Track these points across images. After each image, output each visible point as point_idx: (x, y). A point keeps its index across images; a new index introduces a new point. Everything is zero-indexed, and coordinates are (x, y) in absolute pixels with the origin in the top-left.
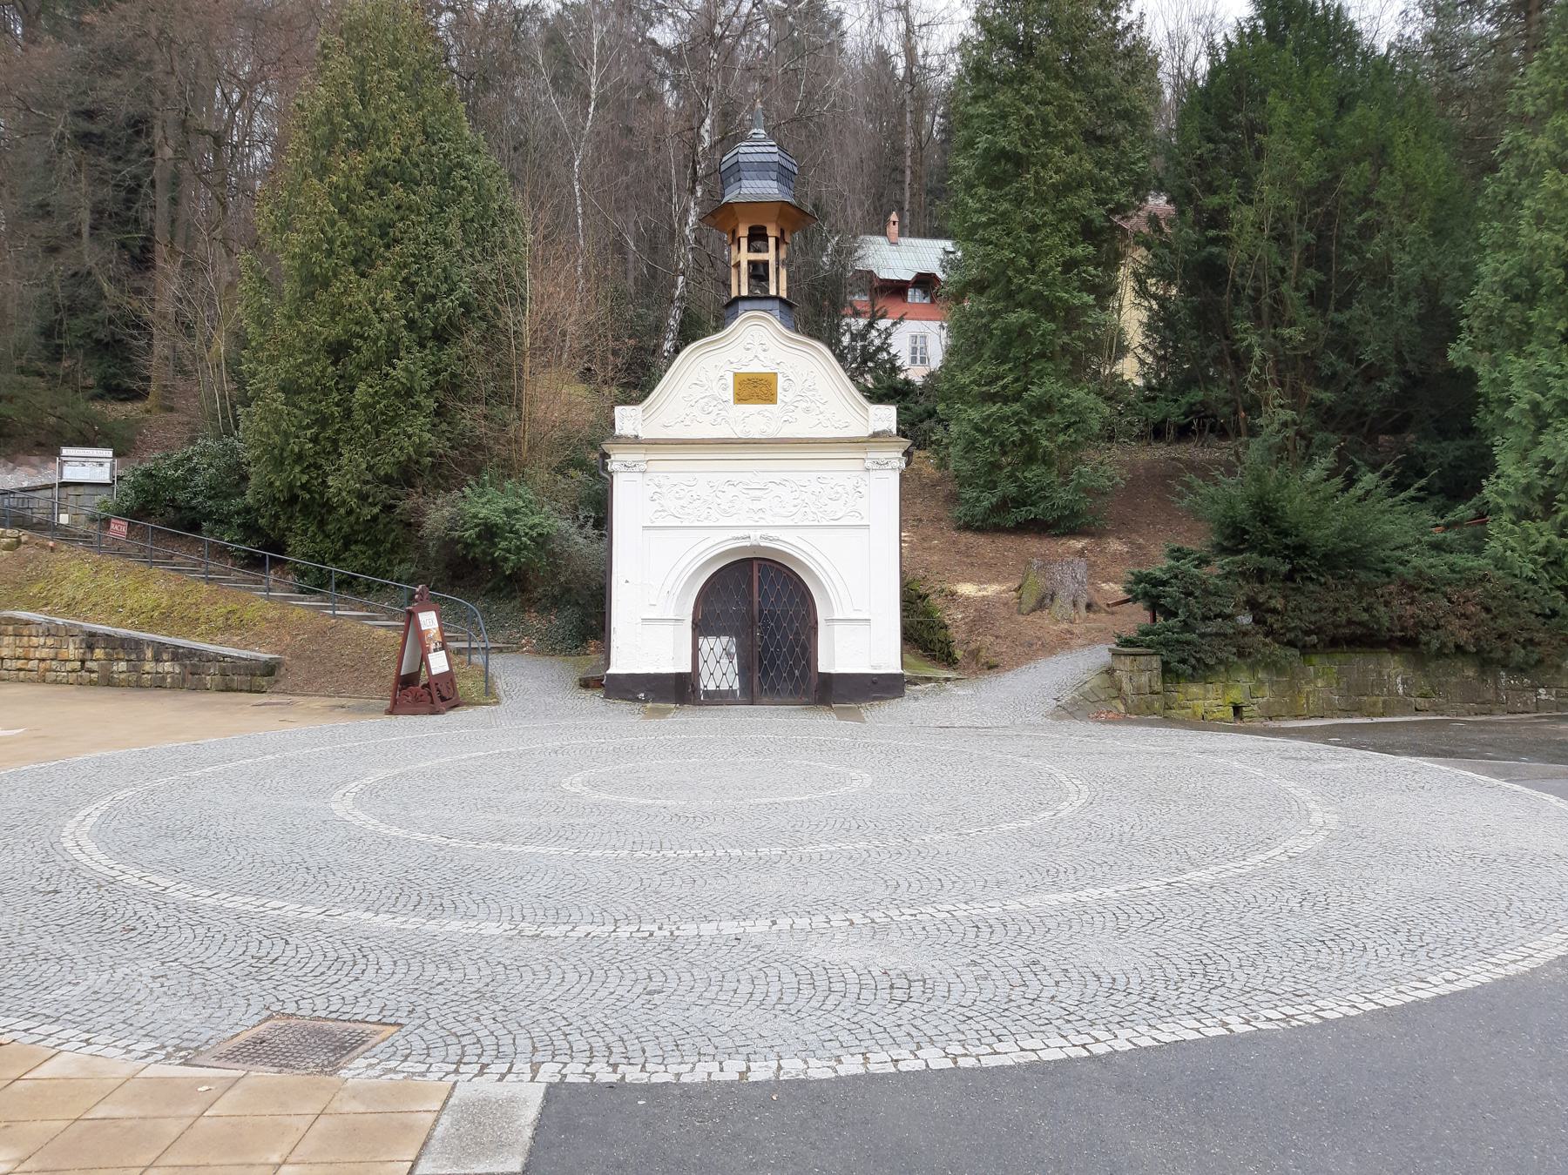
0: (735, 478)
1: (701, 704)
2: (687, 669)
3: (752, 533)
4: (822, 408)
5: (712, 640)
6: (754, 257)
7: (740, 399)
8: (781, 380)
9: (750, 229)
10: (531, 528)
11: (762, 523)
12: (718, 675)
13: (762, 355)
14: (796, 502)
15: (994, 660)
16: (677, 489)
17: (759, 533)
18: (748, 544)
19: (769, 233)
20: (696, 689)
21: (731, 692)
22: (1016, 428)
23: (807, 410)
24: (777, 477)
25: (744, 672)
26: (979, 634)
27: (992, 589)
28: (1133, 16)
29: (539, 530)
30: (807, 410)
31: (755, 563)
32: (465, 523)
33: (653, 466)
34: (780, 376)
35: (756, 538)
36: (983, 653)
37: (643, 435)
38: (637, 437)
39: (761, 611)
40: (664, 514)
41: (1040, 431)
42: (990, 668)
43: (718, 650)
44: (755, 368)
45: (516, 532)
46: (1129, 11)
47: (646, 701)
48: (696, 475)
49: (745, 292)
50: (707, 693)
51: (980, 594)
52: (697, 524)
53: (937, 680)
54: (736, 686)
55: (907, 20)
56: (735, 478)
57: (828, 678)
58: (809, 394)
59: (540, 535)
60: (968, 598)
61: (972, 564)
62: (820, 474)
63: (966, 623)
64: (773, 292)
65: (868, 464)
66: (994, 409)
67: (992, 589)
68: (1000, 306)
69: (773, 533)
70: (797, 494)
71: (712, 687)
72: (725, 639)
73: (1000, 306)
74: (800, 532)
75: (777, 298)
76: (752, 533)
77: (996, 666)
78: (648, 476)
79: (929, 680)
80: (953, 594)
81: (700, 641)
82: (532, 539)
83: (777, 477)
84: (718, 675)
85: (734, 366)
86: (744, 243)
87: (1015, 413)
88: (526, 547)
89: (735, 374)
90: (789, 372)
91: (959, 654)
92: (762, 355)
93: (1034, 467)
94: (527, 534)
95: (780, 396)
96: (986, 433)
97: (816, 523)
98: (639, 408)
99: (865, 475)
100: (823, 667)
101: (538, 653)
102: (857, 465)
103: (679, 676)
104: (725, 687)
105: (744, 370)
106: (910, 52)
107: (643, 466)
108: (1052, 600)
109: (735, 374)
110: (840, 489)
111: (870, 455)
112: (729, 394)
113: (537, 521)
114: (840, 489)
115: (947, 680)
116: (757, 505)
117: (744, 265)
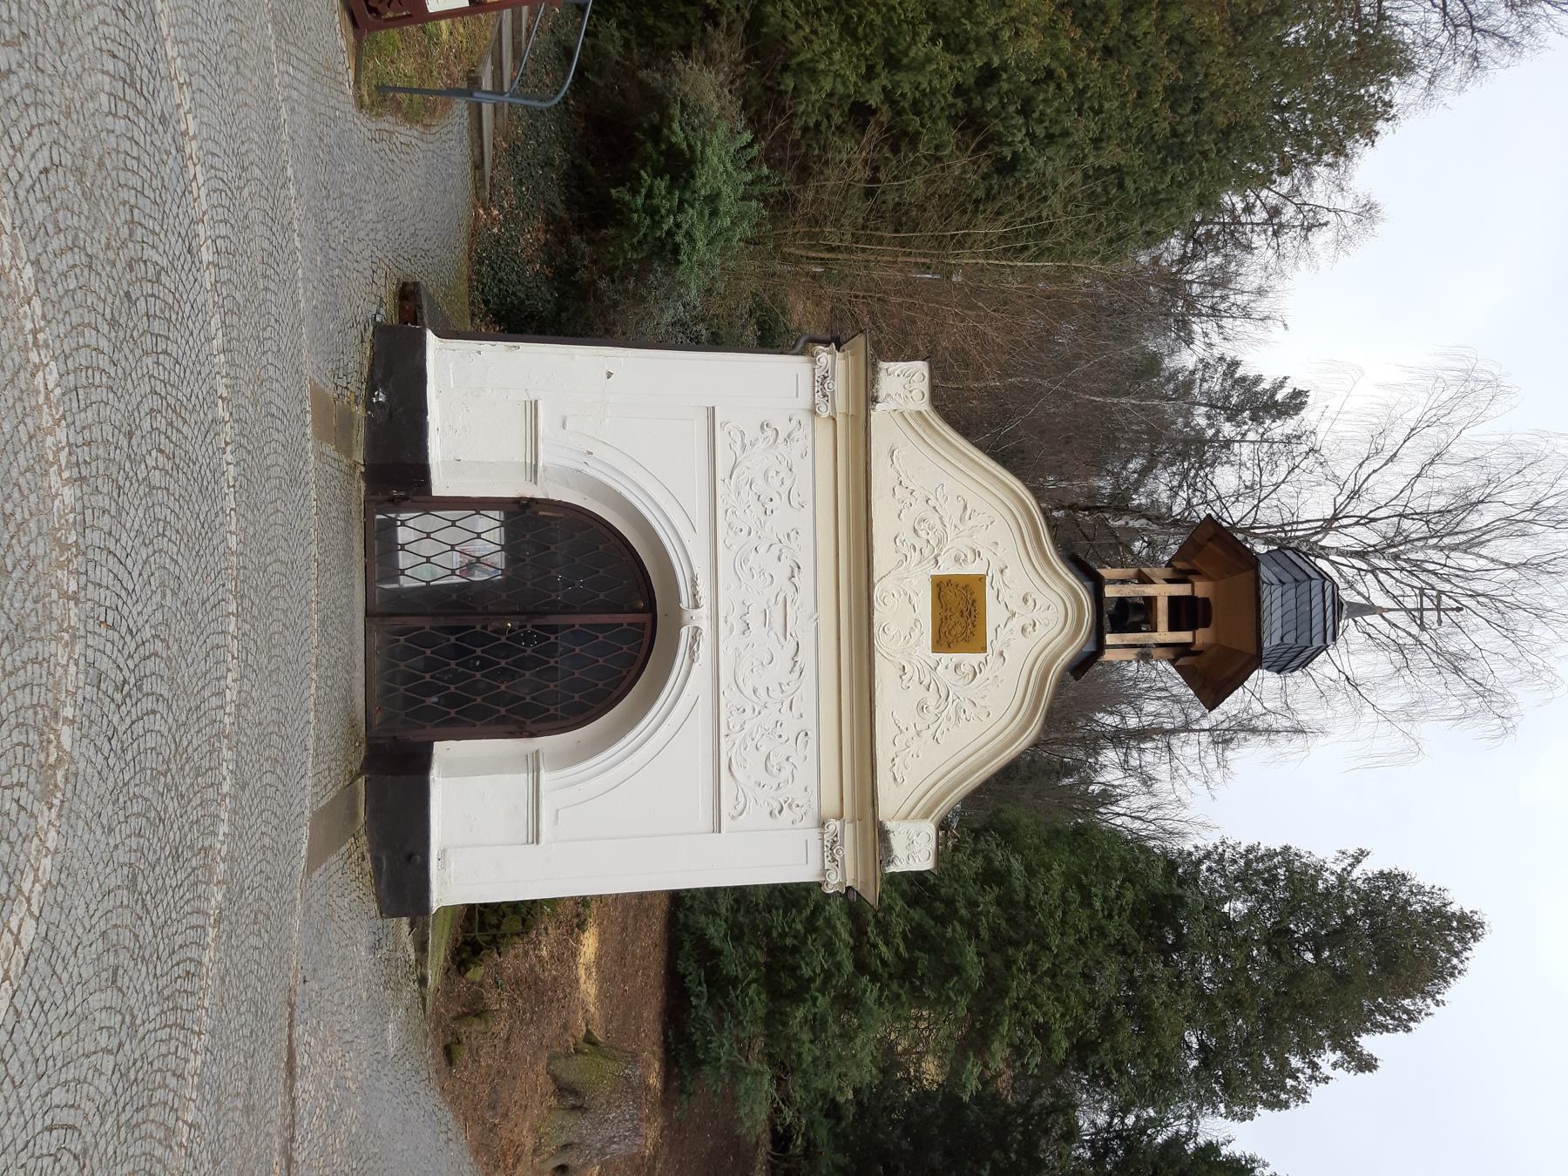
0: (805, 579)
1: (368, 515)
2: (441, 485)
3: (704, 611)
4: (927, 735)
5: (497, 536)
6: (1162, 607)
7: (942, 587)
10: (689, 235)
12: (427, 548)
13: (1016, 624)
14: (762, 692)
15: (463, 1054)
16: (784, 473)
18: (684, 605)
19: (1200, 632)
20: (398, 504)
21: (395, 573)
22: (818, 971)
23: (922, 708)
24: (807, 657)
25: (434, 599)
26: (512, 1001)
27: (589, 988)
28: (1326, 1069)
29: (685, 247)
30: (922, 708)
31: (650, 616)
32: (693, 129)
34: (980, 657)
35: (700, 618)
36: (477, 1026)
37: (878, 413)
38: (875, 400)
39: (553, 629)
40: (738, 448)
41: (814, 1005)
42: (448, 1052)
43: (479, 548)
44: (994, 614)
45: (680, 208)
46: (1334, 1066)
47: (369, 405)
48: (809, 507)
49: (1110, 592)
50: (390, 526)
51: (582, 972)
53: (421, 962)
54: (405, 582)
55: (1174, 732)
56: (805, 579)
57: (415, 765)
58: (951, 709)
59: (676, 249)
60: (574, 954)
61: (624, 929)
62: (812, 735)
63: (532, 968)
64: (1110, 639)
65: (834, 825)
66: (845, 936)
67: (589, 988)
68: (985, 934)
70: (775, 693)
71: (403, 535)
72: (499, 559)
73: (985, 934)
75: (1100, 646)
76: (704, 611)
77: (451, 1062)
78: (806, 419)
79: (422, 947)
80: (582, 926)
81: (496, 514)
82: (670, 233)
83: (807, 657)
84: (427, 548)
85: (997, 576)
86: (1181, 590)
87: (839, 966)
88: (656, 224)
90: (987, 671)
91: (476, 973)
92: (1016, 624)
93: (763, 997)
94: (678, 225)
95: (946, 658)
96: (811, 926)
97: (723, 731)
98: (924, 406)
99: (810, 820)
100: (444, 751)
101: (474, 233)
102: (830, 803)
103: (421, 472)
104: (404, 560)
105: (990, 595)
106: (1142, 734)
107: (825, 412)
108: (574, 1108)
109: (981, 579)
110: (786, 773)
111: (849, 828)
112: (947, 568)
113: (700, 244)
114: (786, 773)
115: (423, 981)
116: (755, 620)
117: (1148, 590)
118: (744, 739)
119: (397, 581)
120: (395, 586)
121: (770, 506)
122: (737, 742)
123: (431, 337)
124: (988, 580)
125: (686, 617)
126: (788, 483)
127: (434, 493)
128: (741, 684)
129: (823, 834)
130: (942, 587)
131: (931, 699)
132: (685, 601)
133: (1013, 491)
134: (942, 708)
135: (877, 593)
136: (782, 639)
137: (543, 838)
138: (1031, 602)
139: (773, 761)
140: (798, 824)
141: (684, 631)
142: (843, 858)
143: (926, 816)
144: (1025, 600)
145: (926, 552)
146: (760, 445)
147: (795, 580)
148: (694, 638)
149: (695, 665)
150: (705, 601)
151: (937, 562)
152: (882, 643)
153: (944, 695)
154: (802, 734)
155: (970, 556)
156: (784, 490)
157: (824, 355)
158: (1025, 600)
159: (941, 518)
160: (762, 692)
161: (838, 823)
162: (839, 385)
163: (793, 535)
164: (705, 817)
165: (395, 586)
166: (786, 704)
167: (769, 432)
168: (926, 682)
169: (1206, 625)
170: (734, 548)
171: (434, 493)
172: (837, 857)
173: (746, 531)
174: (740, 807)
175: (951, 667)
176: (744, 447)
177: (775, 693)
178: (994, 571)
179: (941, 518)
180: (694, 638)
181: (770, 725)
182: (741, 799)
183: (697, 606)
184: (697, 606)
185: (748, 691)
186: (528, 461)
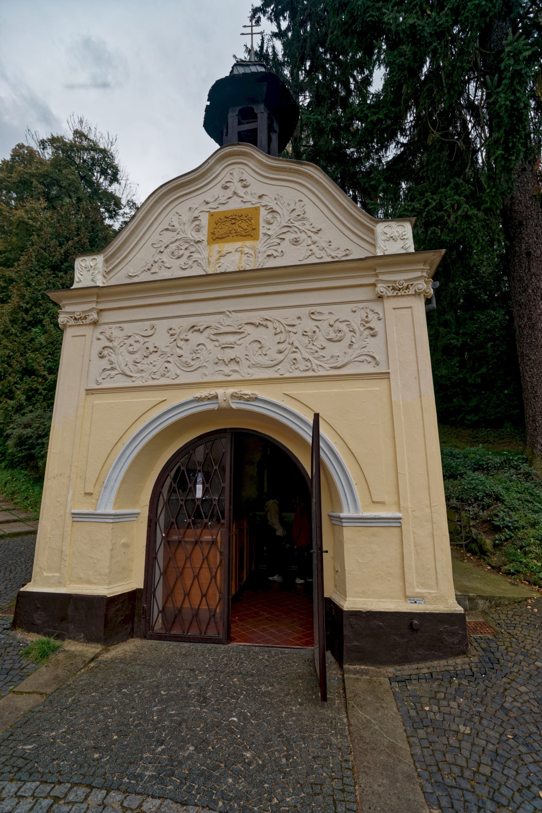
0: (202, 322)
3: (220, 392)
4: (315, 237)
11: (235, 377)
14: (282, 347)
16: (131, 341)
17: (231, 391)
18: (215, 407)
23: (296, 242)
24: (256, 317)
30: (296, 242)
33: (107, 317)
40: (113, 373)
48: (154, 322)
52: (151, 383)
56: (202, 322)
58: (297, 224)
62: (313, 309)
65: (381, 288)
69: (247, 391)
70: (282, 337)
76: (220, 392)
78: (101, 329)
83: (256, 317)
85: (210, 205)
90: (273, 205)
92: (241, 191)
99: (377, 307)
107: (94, 316)
110: (343, 327)
114: (343, 327)
116: (230, 354)
121: (152, 349)
123: (30, 588)
124: (212, 211)
125: (224, 405)
126: (138, 338)
127: (142, 587)
128: (275, 362)
129: (388, 297)
131: (289, 237)
132: (213, 406)
134: (296, 230)
136: (243, 335)
139: (332, 335)
141: (234, 406)
142: (406, 280)
143: (372, 231)
145: (193, 249)
146: (113, 358)
147: (202, 328)
148: (240, 398)
149: (260, 396)
150: (212, 391)
151: (199, 242)
154: (313, 316)
155: (197, 223)
156: (142, 340)
157: (62, 319)
159: (172, 243)
160: (282, 347)
161: (379, 285)
162: (78, 309)
163: (171, 332)
167: (105, 352)
168: (279, 241)
169: (253, 109)
170: (178, 372)
171: (142, 587)
172: (405, 285)
173: (167, 365)
174: (369, 359)
176: (113, 369)
177: (282, 337)
178: (206, 208)
179: (172, 243)
181: (306, 340)
182: (363, 358)
183: (216, 397)
184: (216, 397)
185: (280, 357)
186: (111, 521)
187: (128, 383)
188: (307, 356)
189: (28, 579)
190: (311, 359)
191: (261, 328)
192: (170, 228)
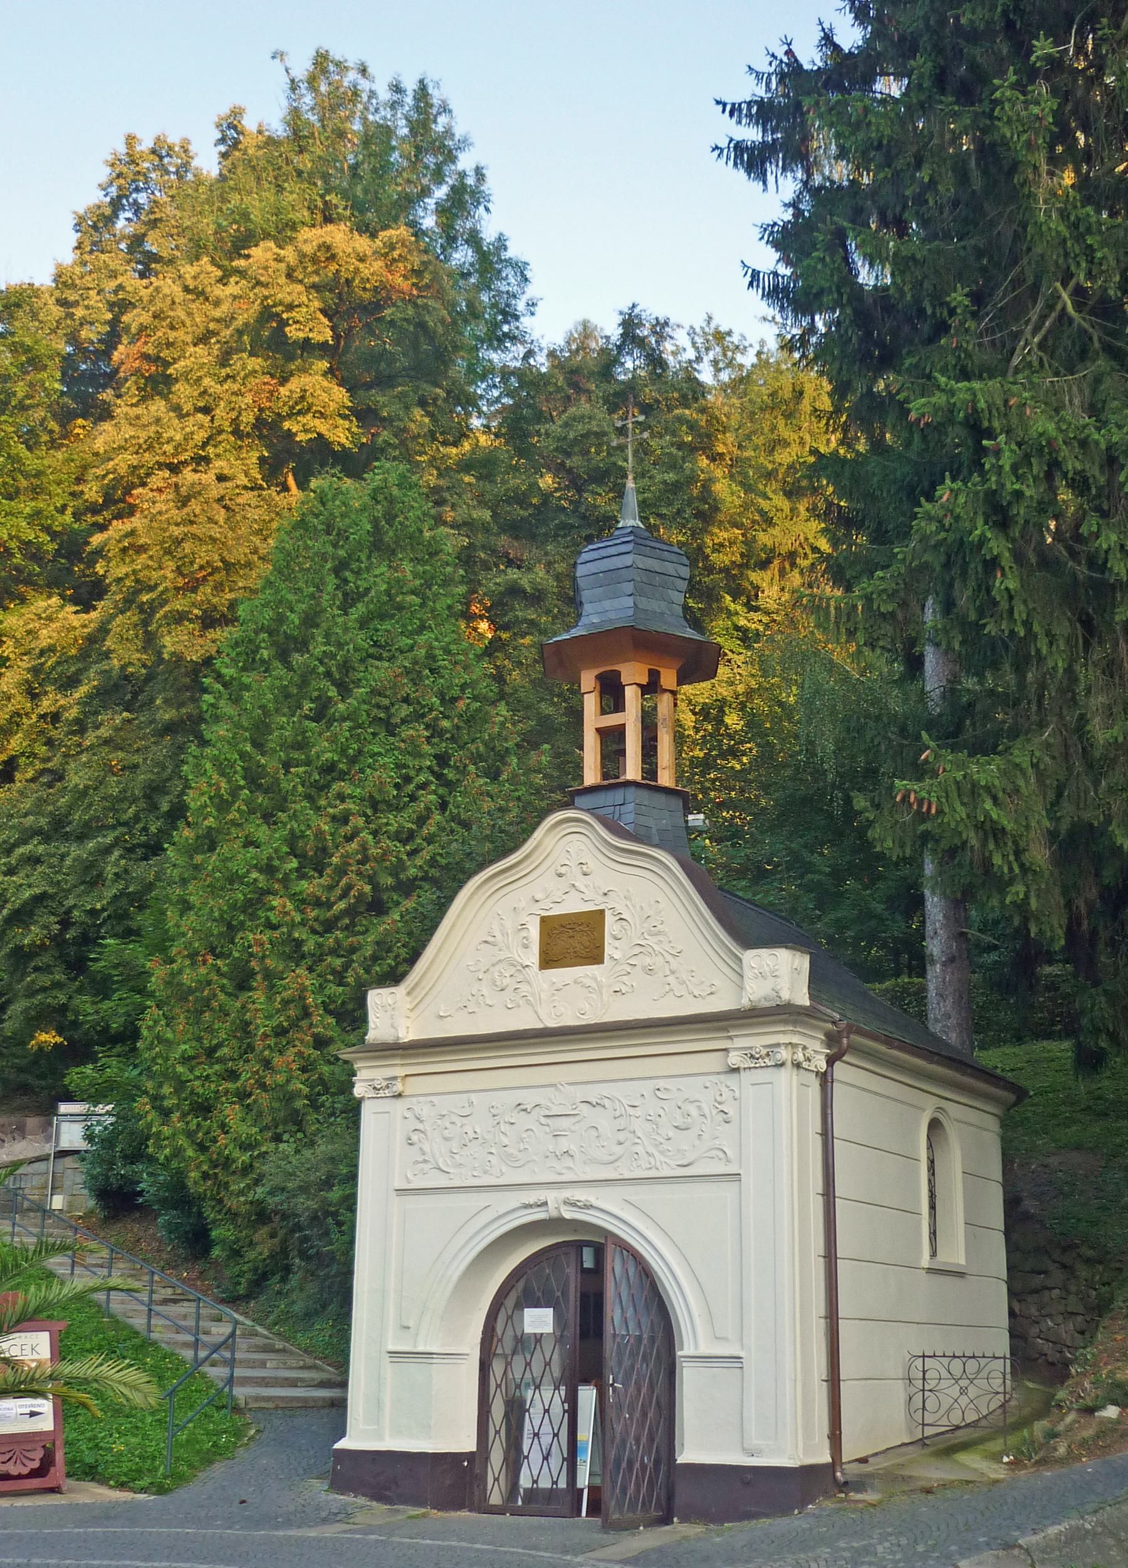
0: (529, 1098)
3: (553, 1197)
4: (674, 964)
7: (548, 961)
8: (609, 919)
9: (598, 677)
14: (621, 1136)
24: (593, 1093)
30: (650, 971)
33: (414, 1086)
34: (608, 914)
44: (573, 905)
48: (473, 1097)
56: (529, 1098)
58: (652, 941)
62: (661, 1083)
65: (734, 1059)
69: (580, 1195)
70: (622, 1122)
74: (629, 1192)
83: (593, 1093)
85: (541, 905)
89: (544, 920)
95: (608, 950)
97: (653, 1173)
98: (401, 990)
99: (732, 1080)
102: (712, 1062)
103: (453, 1459)
109: (544, 920)
111: (739, 1043)
112: (533, 957)
114: (692, 1109)
116: (564, 1144)
118: (662, 1153)
119: (582, 1490)
120: (586, 1492)
121: (471, 1135)
122: (663, 1159)
125: (554, 1214)
126: (454, 1119)
128: (612, 1158)
130: (548, 961)
133: (470, 898)
135: (552, 1024)
136: (577, 1118)
137: (736, 1354)
138: (563, 870)
140: (737, 1095)
141: (567, 1215)
142: (765, 1047)
144: (560, 875)
145: (520, 978)
146: (426, 1147)
147: (529, 1108)
148: (573, 1205)
149: (595, 1203)
152: (570, 1020)
153: (638, 950)
155: (524, 934)
157: (358, 1091)
158: (560, 875)
160: (621, 1136)
163: (494, 1111)
164: (727, 1191)
165: (586, 1492)
166: (630, 1111)
167: (415, 1137)
170: (504, 1169)
173: (490, 1157)
174: (721, 1155)
175: (617, 943)
176: (425, 1161)
177: (622, 1122)
180: (573, 1205)
181: (649, 1127)
182: (714, 1153)
183: (545, 1204)
184: (545, 1204)
185: (619, 1150)
187: (443, 1182)
188: (652, 1150)
189: (341, 1433)
190: (656, 1154)
191: (598, 1108)
192: (490, 939)
